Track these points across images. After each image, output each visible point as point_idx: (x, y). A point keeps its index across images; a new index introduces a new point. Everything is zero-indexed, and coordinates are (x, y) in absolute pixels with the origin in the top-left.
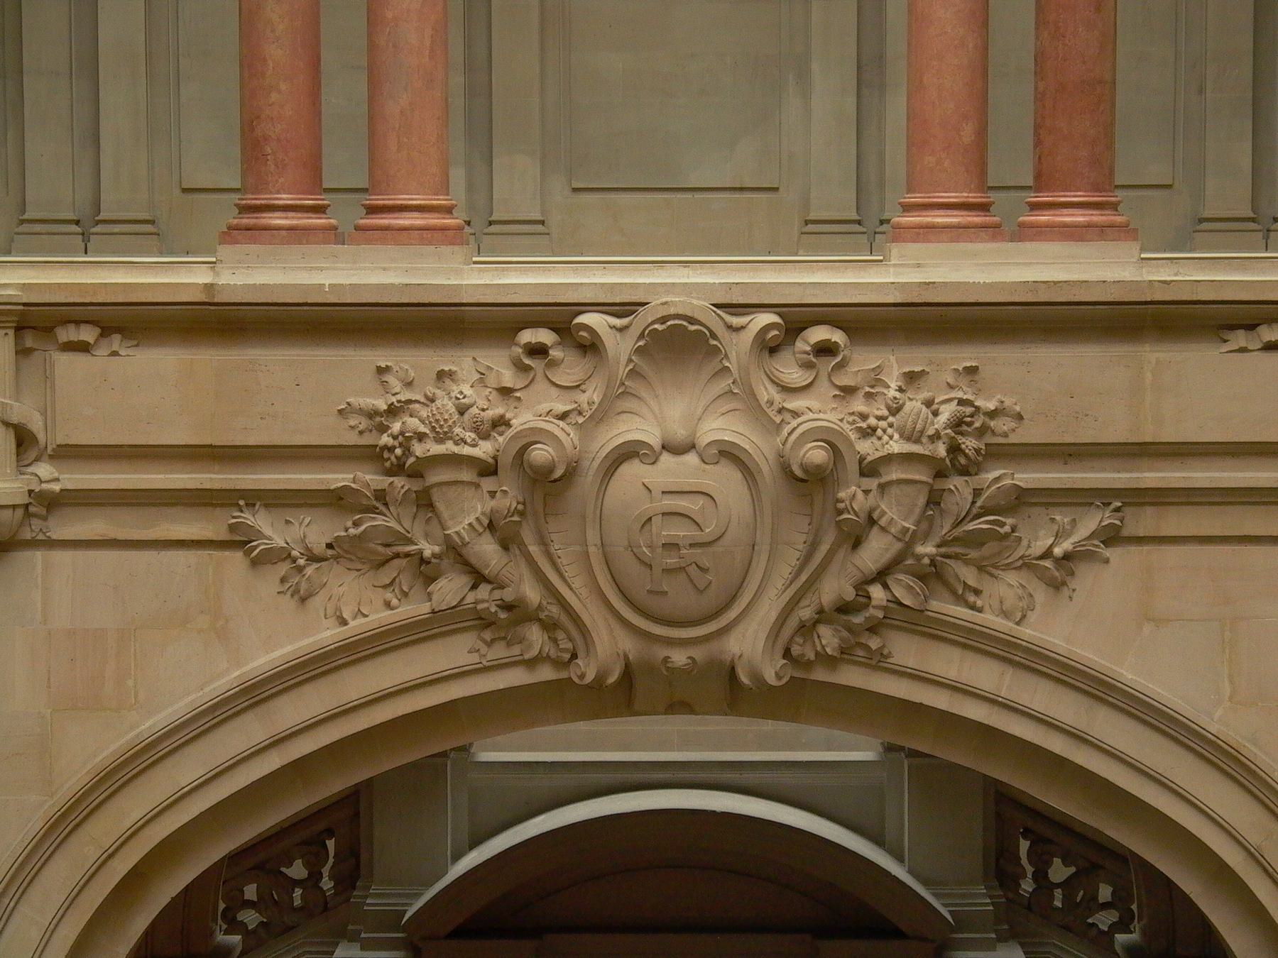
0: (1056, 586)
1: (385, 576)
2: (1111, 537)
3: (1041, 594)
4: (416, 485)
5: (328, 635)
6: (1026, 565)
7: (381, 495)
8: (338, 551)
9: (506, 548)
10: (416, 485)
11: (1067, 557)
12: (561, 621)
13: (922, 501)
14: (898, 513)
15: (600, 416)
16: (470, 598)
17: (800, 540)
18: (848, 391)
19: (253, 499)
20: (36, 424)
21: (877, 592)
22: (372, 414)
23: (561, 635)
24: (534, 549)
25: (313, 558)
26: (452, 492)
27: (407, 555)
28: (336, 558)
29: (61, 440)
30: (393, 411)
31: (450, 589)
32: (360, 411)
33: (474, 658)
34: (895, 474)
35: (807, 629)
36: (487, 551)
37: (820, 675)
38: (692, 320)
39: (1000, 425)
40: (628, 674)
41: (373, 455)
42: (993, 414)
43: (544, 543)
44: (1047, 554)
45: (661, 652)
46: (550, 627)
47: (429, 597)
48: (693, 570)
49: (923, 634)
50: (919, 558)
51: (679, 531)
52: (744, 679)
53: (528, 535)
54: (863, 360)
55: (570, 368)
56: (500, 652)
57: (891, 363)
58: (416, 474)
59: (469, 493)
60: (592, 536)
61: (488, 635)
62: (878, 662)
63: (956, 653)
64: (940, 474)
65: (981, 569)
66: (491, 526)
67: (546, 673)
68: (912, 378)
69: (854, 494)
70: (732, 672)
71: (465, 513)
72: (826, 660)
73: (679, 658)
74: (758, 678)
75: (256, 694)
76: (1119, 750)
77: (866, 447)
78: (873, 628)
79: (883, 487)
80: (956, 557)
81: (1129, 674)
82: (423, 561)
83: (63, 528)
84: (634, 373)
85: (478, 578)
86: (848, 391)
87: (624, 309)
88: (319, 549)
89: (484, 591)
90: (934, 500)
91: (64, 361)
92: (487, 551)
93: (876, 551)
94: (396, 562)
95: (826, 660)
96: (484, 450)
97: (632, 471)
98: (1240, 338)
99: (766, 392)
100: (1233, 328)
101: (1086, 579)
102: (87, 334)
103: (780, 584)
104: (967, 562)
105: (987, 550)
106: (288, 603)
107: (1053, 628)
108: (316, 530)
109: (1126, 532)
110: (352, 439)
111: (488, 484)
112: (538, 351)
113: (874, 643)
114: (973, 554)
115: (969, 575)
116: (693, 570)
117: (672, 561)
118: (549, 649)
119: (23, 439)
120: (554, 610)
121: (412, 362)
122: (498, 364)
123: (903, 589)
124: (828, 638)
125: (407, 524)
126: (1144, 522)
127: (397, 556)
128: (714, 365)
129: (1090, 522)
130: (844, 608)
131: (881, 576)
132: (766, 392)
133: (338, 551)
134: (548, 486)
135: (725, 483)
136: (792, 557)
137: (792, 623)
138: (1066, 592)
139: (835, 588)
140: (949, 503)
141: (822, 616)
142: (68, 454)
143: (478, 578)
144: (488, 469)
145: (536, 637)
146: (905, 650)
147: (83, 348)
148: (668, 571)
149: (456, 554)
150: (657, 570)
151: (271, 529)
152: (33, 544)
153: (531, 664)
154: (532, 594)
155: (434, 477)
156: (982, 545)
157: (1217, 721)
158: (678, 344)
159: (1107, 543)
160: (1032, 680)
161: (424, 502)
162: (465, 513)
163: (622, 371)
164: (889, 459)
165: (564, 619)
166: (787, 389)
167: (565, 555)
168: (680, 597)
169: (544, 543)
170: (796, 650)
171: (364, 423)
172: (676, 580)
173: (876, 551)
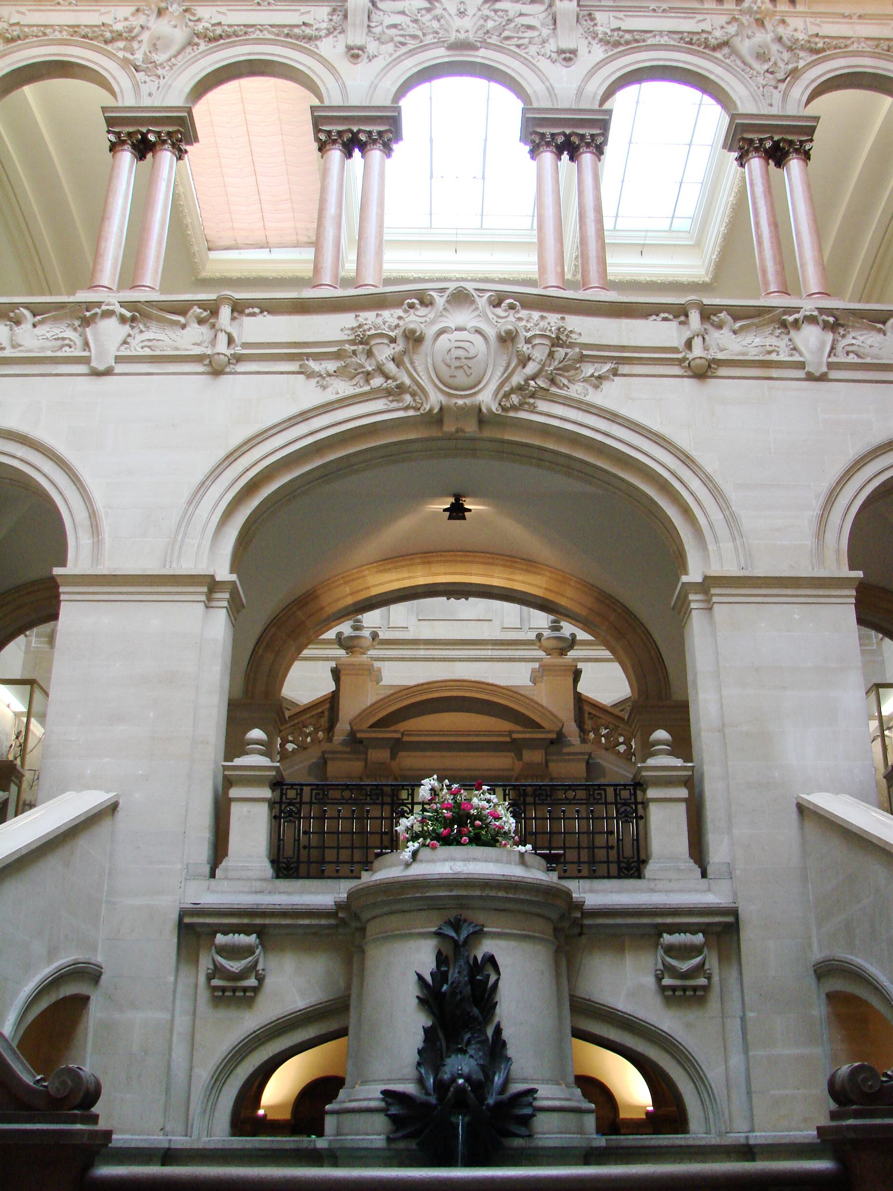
0: (596, 387)
1: (354, 382)
2: (615, 374)
3: (591, 390)
4: (367, 347)
5: (333, 397)
6: (585, 380)
7: (354, 353)
8: (336, 374)
9: (398, 367)
10: (367, 347)
11: (600, 377)
12: (418, 391)
13: (547, 351)
14: (539, 354)
15: (433, 322)
16: (385, 385)
17: (504, 363)
18: (520, 319)
19: (308, 356)
20: (235, 335)
21: (532, 383)
22: (352, 329)
23: (417, 398)
24: (408, 365)
25: (329, 375)
26: (380, 347)
27: (362, 372)
28: (337, 376)
29: (243, 341)
30: (360, 326)
31: (377, 382)
32: (349, 329)
33: (386, 407)
34: (537, 341)
35: (507, 395)
36: (391, 367)
37: (511, 414)
38: (466, 290)
39: (573, 336)
40: (441, 409)
41: (353, 342)
42: (571, 332)
43: (412, 363)
44: (592, 376)
45: (454, 401)
46: (413, 395)
47: (369, 384)
48: (466, 367)
49: (549, 400)
50: (546, 371)
51: (461, 353)
52: (484, 410)
53: (406, 360)
54: (524, 313)
55: (422, 311)
56: (395, 405)
57: (536, 315)
58: (367, 344)
59: (386, 347)
60: (430, 360)
61: (391, 398)
62: (533, 410)
63: (562, 407)
64: (553, 346)
65: (569, 381)
66: (393, 360)
67: (411, 413)
68: (542, 318)
69: (525, 348)
70: (480, 410)
71: (384, 353)
72: (514, 408)
73: (460, 402)
74: (489, 410)
75: (304, 416)
76: (621, 438)
77: (529, 335)
78: (533, 395)
79: (533, 347)
80: (560, 375)
81: (624, 411)
82: (368, 373)
83: (241, 368)
84: (445, 309)
85: (387, 377)
86: (520, 319)
87: (442, 290)
88: (331, 372)
89: (390, 381)
90: (551, 355)
91: (246, 320)
92: (391, 367)
93: (531, 368)
94: (358, 376)
95: (514, 408)
96: (392, 334)
97: (444, 337)
98: (654, 317)
99: (491, 316)
100: (651, 315)
101: (606, 385)
102: (257, 310)
103: (497, 378)
104: (564, 377)
105: (572, 373)
106: (319, 390)
107: (595, 397)
108: (331, 366)
109: (619, 372)
110: (346, 338)
111: (392, 345)
112: (412, 306)
113: (531, 401)
114: (566, 374)
115: (565, 382)
116: (466, 367)
117: (458, 364)
118: (413, 404)
119: (231, 341)
120: (415, 388)
121: (369, 317)
122: (399, 312)
123: (541, 383)
124: (515, 399)
125: (363, 360)
126: (624, 369)
127: (359, 374)
128: (473, 307)
129: (607, 367)
130: (520, 388)
131: (533, 378)
132: (491, 316)
133: (336, 374)
134: (414, 339)
135: (478, 339)
136: (502, 369)
137: (502, 393)
138: (599, 390)
139: (517, 379)
140: (557, 355)
141: (512, 391)
142: (245, 345)
143: (387, 377)
144: (393, 340)
145: (408, 398)
146: (542, 406)
147: (253, 315)
148: (457, 368)
149: (380, 370)
150: (453, 367)
151: (313, 365)
152: (231, 373)
153: (407, 408)
154: (407, 381)
155: (373, 342)
156: (569, 368)
157: (656, 427)
158: (460, 298)
159: (614, 375)
160: (589, 416)
161: (370, 354)
162: (384, 353)
163: (441, 308)
164: (535, 336)
165: (419, 391)
166: (499, 317)
167: (419, 369)
168: (461, 379)
169: (412, 363)
170: (503, 404)
171: (349, 332)
172: (459, 373)
173: (531, 368)
